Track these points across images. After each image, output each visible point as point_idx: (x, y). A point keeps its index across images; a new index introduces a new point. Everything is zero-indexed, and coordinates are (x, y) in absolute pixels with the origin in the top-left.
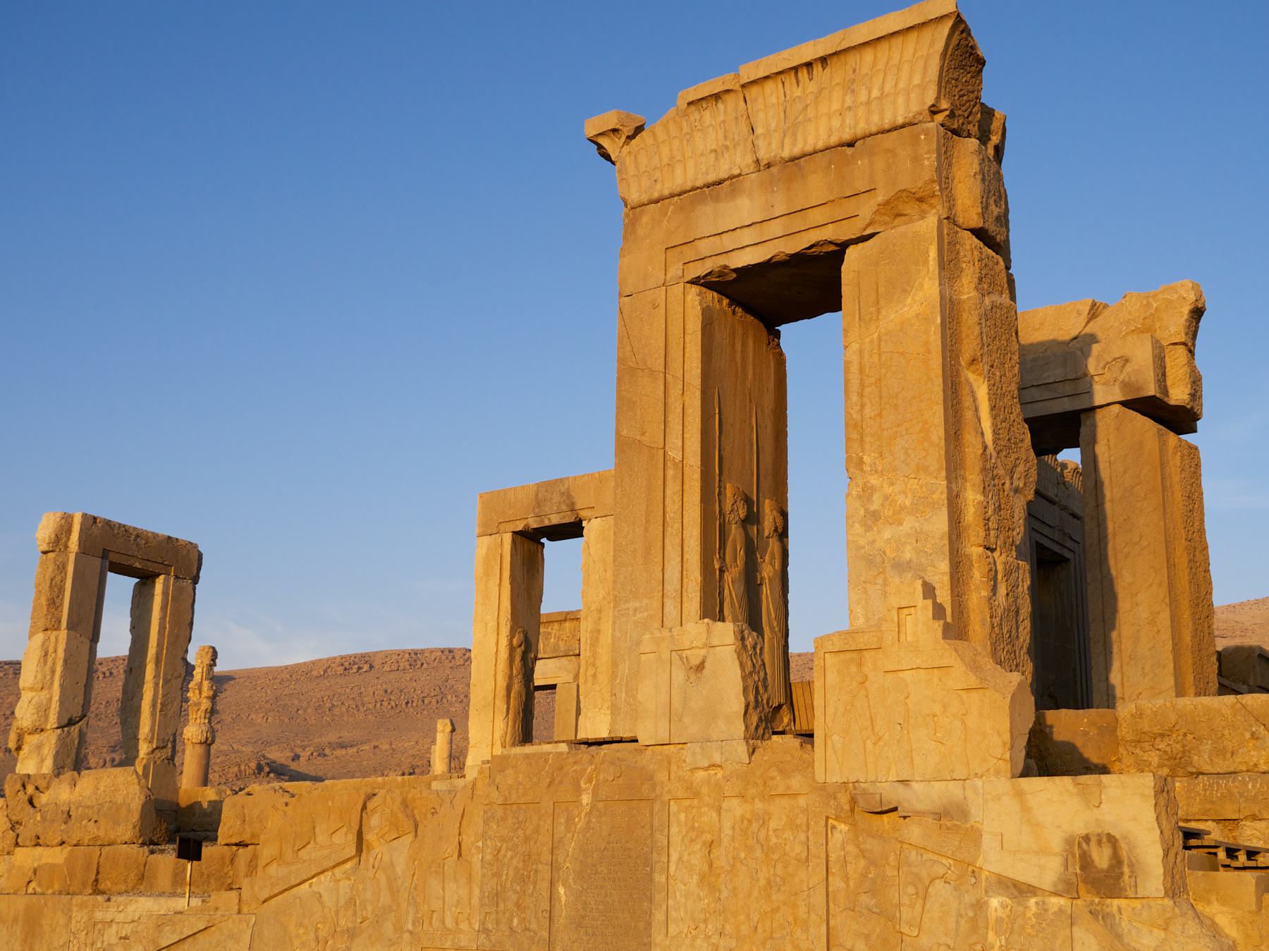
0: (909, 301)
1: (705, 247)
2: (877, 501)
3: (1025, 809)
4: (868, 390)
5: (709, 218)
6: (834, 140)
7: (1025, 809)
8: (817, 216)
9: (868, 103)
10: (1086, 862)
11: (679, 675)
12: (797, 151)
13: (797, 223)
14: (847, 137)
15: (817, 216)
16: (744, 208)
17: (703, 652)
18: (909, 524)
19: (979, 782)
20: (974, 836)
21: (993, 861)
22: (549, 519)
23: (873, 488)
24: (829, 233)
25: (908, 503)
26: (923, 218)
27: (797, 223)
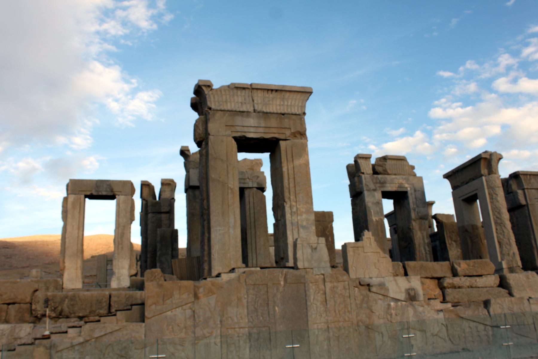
0: (301, 159)
1: (238, 129)
2: (294, 209)
3: (397, 284)
4: (291, 180)
5: (239, 121)
6: (279, 112)
7: (397, 284)
8: (274, 130)
9: (287, 105)
10: (409, 294)
11: (309, 251)
12: (268, 111)
13: (267, 130)
14: (283, 112)
15: (274, 130)
16: (251, 121)
17: (316, 245)
18: (304, 216)
19: (387, 278)
20: (387, 290)
21: (392, 294)
22: (102, 193)
23: (294, 206)
24: (276, 136)
25: (304, 210)
26: (301, 139)
27: (267, 130)
